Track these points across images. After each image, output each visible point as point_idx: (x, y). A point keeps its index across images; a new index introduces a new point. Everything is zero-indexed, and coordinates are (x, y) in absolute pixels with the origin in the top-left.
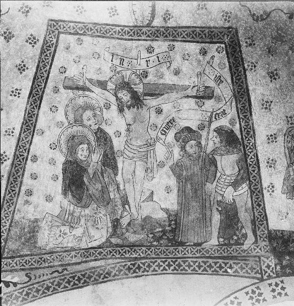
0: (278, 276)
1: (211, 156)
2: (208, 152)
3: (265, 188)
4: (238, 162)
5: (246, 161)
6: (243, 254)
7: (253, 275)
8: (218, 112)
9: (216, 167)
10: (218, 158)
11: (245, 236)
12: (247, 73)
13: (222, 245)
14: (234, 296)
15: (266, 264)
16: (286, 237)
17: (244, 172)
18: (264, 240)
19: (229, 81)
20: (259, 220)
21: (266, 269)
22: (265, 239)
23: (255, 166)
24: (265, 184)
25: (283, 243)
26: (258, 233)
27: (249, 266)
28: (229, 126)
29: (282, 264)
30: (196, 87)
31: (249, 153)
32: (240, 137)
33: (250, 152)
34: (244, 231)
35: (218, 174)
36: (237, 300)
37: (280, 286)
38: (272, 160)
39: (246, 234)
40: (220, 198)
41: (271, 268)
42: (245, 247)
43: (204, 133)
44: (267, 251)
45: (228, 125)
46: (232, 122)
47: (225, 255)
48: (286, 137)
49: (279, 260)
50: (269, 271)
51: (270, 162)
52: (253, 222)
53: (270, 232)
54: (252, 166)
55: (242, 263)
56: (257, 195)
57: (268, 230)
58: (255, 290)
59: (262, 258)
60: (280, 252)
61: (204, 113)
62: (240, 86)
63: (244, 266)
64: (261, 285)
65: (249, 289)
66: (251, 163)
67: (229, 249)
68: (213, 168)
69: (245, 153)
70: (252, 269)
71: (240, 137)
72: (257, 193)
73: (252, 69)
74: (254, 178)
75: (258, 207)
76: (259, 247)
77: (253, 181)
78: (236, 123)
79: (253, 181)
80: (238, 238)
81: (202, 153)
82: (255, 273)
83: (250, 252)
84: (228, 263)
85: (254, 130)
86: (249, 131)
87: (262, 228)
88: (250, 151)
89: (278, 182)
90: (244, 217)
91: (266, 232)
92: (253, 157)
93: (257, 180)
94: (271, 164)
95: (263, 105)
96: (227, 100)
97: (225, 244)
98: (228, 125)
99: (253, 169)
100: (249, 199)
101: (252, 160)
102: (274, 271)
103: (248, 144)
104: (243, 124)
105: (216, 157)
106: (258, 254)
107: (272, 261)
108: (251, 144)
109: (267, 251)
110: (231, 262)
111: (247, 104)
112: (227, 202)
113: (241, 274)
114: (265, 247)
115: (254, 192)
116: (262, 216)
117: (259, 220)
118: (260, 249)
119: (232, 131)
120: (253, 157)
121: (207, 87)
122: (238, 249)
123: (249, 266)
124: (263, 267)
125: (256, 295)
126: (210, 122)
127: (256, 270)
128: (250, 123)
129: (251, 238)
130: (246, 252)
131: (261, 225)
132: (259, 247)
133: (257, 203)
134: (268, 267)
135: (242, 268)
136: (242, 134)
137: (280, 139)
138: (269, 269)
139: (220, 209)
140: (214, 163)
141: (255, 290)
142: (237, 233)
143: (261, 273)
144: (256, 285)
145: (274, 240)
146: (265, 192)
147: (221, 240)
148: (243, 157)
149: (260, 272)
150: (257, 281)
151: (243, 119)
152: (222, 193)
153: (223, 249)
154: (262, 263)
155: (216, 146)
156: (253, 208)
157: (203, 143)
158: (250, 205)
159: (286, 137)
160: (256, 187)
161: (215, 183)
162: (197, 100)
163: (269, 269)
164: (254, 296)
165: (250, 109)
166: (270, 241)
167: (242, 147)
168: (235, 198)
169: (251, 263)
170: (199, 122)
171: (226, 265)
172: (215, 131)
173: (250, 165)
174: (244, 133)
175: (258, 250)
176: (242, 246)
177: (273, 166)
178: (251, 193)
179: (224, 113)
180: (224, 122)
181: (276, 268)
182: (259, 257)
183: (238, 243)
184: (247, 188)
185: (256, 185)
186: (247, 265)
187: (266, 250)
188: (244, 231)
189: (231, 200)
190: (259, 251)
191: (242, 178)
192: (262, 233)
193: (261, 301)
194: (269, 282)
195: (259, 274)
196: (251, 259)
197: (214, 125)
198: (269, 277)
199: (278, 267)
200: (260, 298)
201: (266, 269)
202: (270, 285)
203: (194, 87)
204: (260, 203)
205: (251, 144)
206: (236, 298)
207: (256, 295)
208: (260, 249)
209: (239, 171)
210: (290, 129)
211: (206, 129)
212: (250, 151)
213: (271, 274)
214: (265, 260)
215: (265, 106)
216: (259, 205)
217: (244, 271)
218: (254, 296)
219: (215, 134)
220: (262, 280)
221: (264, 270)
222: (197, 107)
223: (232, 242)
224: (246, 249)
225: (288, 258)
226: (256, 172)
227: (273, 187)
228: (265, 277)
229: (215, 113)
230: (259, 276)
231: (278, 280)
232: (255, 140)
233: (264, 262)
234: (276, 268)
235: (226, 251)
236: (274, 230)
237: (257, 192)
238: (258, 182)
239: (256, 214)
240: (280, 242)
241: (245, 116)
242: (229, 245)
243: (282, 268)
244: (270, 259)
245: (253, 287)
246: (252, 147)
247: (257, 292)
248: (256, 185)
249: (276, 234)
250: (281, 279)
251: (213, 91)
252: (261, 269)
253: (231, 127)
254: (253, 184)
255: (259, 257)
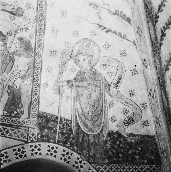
0: (38, 141)
1: (11, 55)
2: (10, 52)
3: (42, 85)
4: (29, 63)
5: (34, 64)
6: (19, 124)
7: (21, 138)
8: (23, 27)
9: (13, 63)
10: (16, 57)
11: (22, 112)
12: (48, 7)
13: (5, 116)
14: (4, 151)
15: (32, 133)
16: (48, 118)
17: (31, 71)
18: (34, 117)
19: (35, 9)
20: (34, 104)
21: (31, 136)
22: (35, 117)
23: (39, 69)
24: (43, 82)
25: (46, 121)
26: (32, 112)
27: (20, 133)
28: (28, 38)
29: (42, 134)
30: (12, 6)
31: (37, 60)
32: (33, 48)
33: (38, 59)
34: (22, 109)
35: (14, 69)
36: (6, 154)
37: (38, 148)
38: (51, 68)
39: (23, 111)
40: (11, 84)
41: (34, 136)
42: (20, 120)
43: (10, 38)
44: (35, 125)
45: (28, 37)
46: (31, 36)
47: (6, 123)
48: (62, 55)
49: (41, 131)
50: (33, 138)
51: (49, 68)
52: (30, 105)
53: (39, 113)
54: (37, 68)
55: (16, 130)
56: (36, 87)
57: (38, 112)
58: (21, 148)
59: (30, 129)
60: (42, 126)
61: (14, 25)
62: (41, 14)
63: (17, 132)
64: (25, 146)
65: (17, 148)
66: (37, 66)
67: (9, 119)
68: (11, 63)
69: (35, 59)
70: (22, 135)
71: (33, 48)
72: (36, 85)
73: (51, 6)
74: (37, 76)
75: (35, 96)
76: (30, 121)
77: (36, 78)
78: (33, 37)
79: (36, 78)
80: (18, 114)
81: (5, 52)
82: (24, 138)
83: (23, 123)
84: (6, 129)
85: (43, 45)
86: (40, 44)
87: (35, 109)
88: (38, 58)
89: (51, 83)
90: (25, 100)
91: (37, 112)
92: (39, 62)
93: (38, 78)
94: (49, 70)
95: (53, 31)
96: (31, 21)
97: (7, 116)
98: (28, 37)
99: (38, 70)
100: (31, 89)
101: (38, 64)
102: (36, 138)
103: (38, 54)
104: (37, 40)
105: (15, 56)
106: (28, 126)
107: (36, 131)
108: (40, 54)
109: (35, 125)
110: (9, 128)
111: (43, 27)
112: (15, 88)
113: (14, 137)
114: (34, 122)
115: (35, 85)
116: (36, 102)
117: (34, 104)
118: (30, 123)
119: (30, 42)
120: (39, 62)
121: (19, 8)
122: (15, 120)
123: (20, 133)
124: (30, 135)
125: (20, 152)
126: (16, 32)
127: (24, 136)
128: (42, 40)
129: (26, 114)
130: (21, 123)
131: (35, 107)
132: (30, 121)
133: (35, 93)
134: (33, 135)
135: (15, 133)
136: (35, 46)
137: (59, 55)
138: (33, 136)
139: (9, 91)
140: (12, 60)
141: (21, 148)
142: (18, 109)
143: (27, 139)
144: (22, 146)
145: (40, 118)
146: (41, 86)
147: (5, 112)
148: (33, 61)
149: (27, 137)
150: (24, 143)
151: (38, 37)
152: (14, 81)
153: (5, 118)
154: (30, 131)
155: (17, 49)
156: (32, 94)
157: (8, 45)
158: (30, 93)
159: (62, 55)
160: (36, 82)
161: (10, 74)
162: (11, 15)
163: (33, 136)
164: (19, 153)
165: (44, 31)
166: (38, 119)
167: (33, 55)
168: (21, 86)
169: (22, 131)
170: (9, 30)
171: (4, 130)
172: (18, 39)
173: (36, 67)
174: (37, 45)
175: (29, 123)
176: (19, 119)
177: (50, 71)
178: (33, 85)
179: (27, 29)
180: (25, 35)
181: (37, 136)
182: (28, 128)
183: (16, 116)
184: (31, 82)
185: (37, 81)
186: (19, 132)
187: (34, 124)
188: (22, 109)
189: (19, 87)
190: (30, 124)
191: (29, 75)
192: (34, 112)
193: (23, 157)
194: (31, 144)
195: (26, 138)
196: (22, 128)
197: (19, 35)
198: (32, 141)
199: (39, 136)
200: (22, 154)
201: (31, 136)
202: (31, 146)
203: (11, 5)
204: (37, 93)
205: (40, 54)
206: (6, 153)
207: (20, 152)
208: (30, 123)
209: (28, 70)
210: (66, 50)
211: (12, 36)
212: (38, 58)
213: (34, 139)
214: (32, 130)
215: (54, 32)
216: (36, 94)
217: (16, 135)
218: (19, 153)
219: (18, 40)
220: (26, 142)
221: (30, 136)
222: (10, 20)
223: (13, 115)
224: (21, 121)
225: (47, 131)
226: (39, 73)
227: (47, 85)
228: (29, 141)
229: (21, 27)
230: (26, 140)
231: (37, 144)
232: (43, 52)
233: (31, 131)
234: (37, 136)
235: (7, 120)
236: (42, 112)
237: (36, 85)
238: (38, 80)
239: (33, 100)
240: (44, 120)
241: (40, 35)
242: (11, 116)
243: (42, 136)
244: (35, 130)
245: (20, 147)
246: (40, 56)
247: (21, 151)
248: (37, 81)
249: (43, 115)
250: (39, 143)
251: (23, 12)
252: (28, 136)
253: (29, 39)
254: (35, 80)
255: (28, 128)
